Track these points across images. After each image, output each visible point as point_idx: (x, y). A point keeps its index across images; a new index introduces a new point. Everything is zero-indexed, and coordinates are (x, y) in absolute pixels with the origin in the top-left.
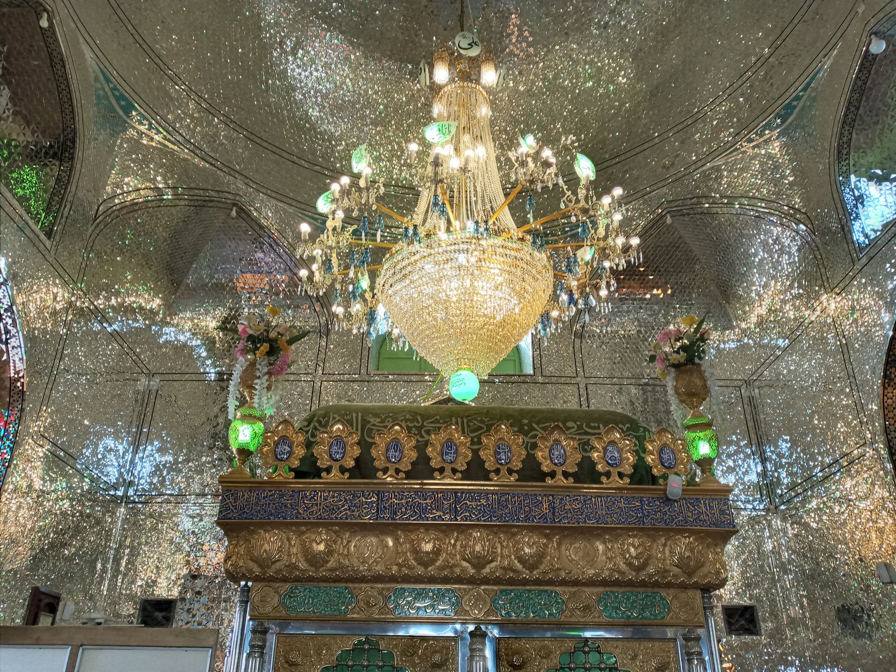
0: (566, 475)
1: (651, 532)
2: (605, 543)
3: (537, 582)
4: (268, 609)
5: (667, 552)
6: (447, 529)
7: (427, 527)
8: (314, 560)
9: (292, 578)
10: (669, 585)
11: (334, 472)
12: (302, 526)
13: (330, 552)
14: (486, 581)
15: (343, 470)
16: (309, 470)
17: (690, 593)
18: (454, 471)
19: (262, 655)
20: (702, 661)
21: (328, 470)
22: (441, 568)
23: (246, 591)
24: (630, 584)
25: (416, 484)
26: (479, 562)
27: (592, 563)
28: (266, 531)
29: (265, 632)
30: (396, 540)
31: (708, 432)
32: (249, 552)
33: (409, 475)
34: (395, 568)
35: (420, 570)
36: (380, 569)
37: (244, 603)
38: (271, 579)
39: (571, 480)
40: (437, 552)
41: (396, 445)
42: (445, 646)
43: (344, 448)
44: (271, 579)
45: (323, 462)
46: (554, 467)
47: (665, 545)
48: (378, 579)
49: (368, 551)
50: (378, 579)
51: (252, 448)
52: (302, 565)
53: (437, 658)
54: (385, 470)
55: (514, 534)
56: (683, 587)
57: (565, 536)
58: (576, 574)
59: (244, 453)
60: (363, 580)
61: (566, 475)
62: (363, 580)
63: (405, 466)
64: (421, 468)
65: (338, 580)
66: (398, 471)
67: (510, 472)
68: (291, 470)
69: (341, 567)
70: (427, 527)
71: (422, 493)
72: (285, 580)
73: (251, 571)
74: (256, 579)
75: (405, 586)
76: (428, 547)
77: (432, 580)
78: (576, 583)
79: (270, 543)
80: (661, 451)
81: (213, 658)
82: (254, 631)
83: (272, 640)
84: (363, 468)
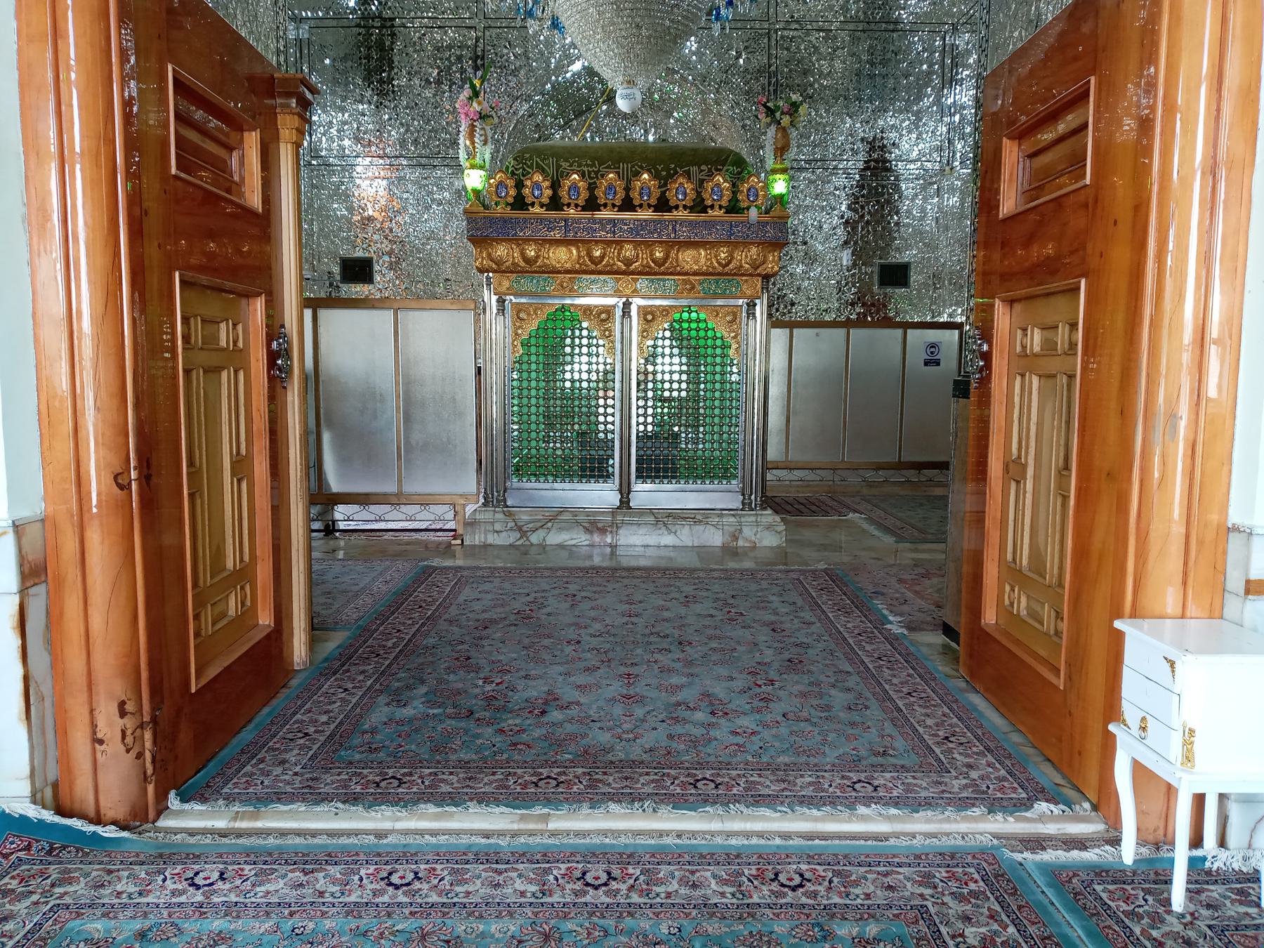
0: (685, 207)
1: (733, 245)
3: (663, 274)
4: (504, 289)
6: (608, 243)
7: (597, 242)
8: (527, 260)
9: (514, 270)
10: (743, 275)
11: (536, 206)
12: (521, 242)
13: (538, 257)
14: (633, 273)
16: (520, 203)
17: (755, 279)
18: (614, 206)
20: (754, 317)
22: (606, 266)
23: (488, 278)
24: (719, 274)
25: (587, 215)
26: (628, 262)
27: (696, 262)
30: (578, 248)
32: (489, 255)
33: (584, 209)
36: (568, 266)
37: (489, 285)
38: (504, 272)
40: (603, 257)
42: (609, 311)
45: (529, 200)
48: (567, 272)
49: (561, 256)
50: (567, 272)
51: (480, 188)
52: (522, 264)
53: (603, 316)
54: (569, 205)
56: (751, 275)
58: (687, 267)
62: (559, 272)
63: (581, 202)
64: (592, 204)
65: (544, 272)
66: (577, 206)
67: (649, 206)
68: (508, 204)
69: (545, 265)
70: (597, 242)
71: (594, 221)
72: (512, 272)
74: (494, 271)
75: (584, 276)
76: (598, 254)
77: (600, 273)
78: (686, 274)
79: (501, 251)
80: (749, 190)
82: (498, 301)
84: (555, 203)
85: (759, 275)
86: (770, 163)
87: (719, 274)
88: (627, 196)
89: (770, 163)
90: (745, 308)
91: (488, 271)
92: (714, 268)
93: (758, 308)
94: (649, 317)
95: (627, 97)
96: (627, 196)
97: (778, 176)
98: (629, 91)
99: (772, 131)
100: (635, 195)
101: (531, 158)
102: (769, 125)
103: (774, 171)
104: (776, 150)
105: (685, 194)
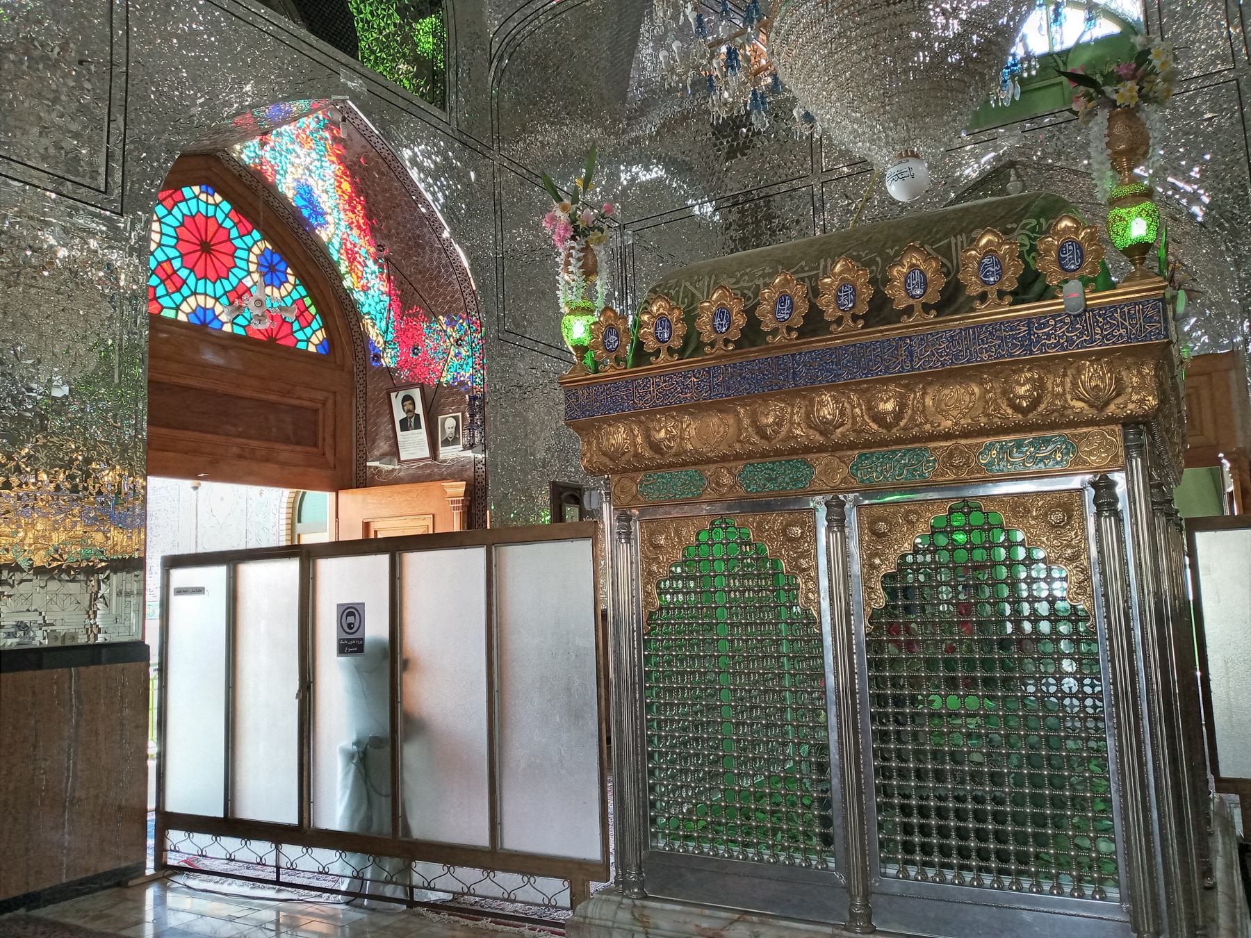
0: (926, 308)
2: (982, 384)
3: (899, 441)
5: (1068, 386)
15: (671, 351)
19: (628, 541)
21: (657, 353)
28: (610, 425)
29: (629, 519)
31: (1147, 205)
34: (738, 447)
35: (765, 445)
39: (933, 313)
41: (723, 312)
43: (670, 327)
44: (625, 471)
46: (911, 302)
47: (1065, 375)
55: (867, 390)
56: (1091, 423)
57: (930, 383)
59: (581, 349)
60: (709, 461)
61: (926, 308)
62: (709, 461)
73: (605, 465)
74: (613, 472)
78: (948, 436)
79: (618, 436)
81: (594, 545)
83: (636, 527)
85: (1112, 420)
86: (1106, 185)
87: (1018, 429)
88: (813, 306)
89: (1106, 185)
90: (1090, 493)
91: (602, 472)
92: (1005, 418)
93: (1121, 489)
94: (882, 527)
95: (900, 176)
96: (813, 306)
97: (1123, 212)
98: (904, 167)
99: (1099, 125)
100: (825, 301)
101: (678, 284)
102: (1091, 114)
103: (1114, 202)
104: (1115, 157)
105: (925, 284)
